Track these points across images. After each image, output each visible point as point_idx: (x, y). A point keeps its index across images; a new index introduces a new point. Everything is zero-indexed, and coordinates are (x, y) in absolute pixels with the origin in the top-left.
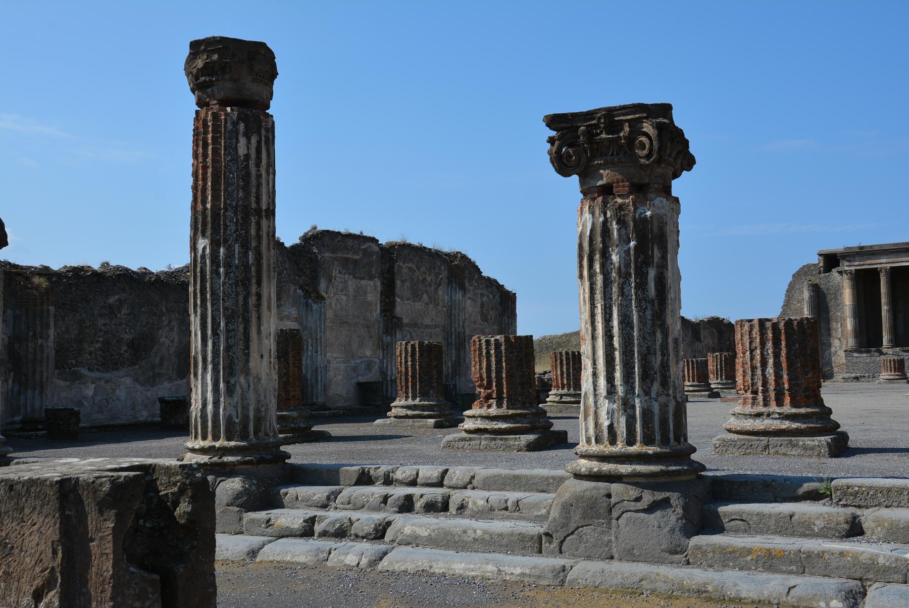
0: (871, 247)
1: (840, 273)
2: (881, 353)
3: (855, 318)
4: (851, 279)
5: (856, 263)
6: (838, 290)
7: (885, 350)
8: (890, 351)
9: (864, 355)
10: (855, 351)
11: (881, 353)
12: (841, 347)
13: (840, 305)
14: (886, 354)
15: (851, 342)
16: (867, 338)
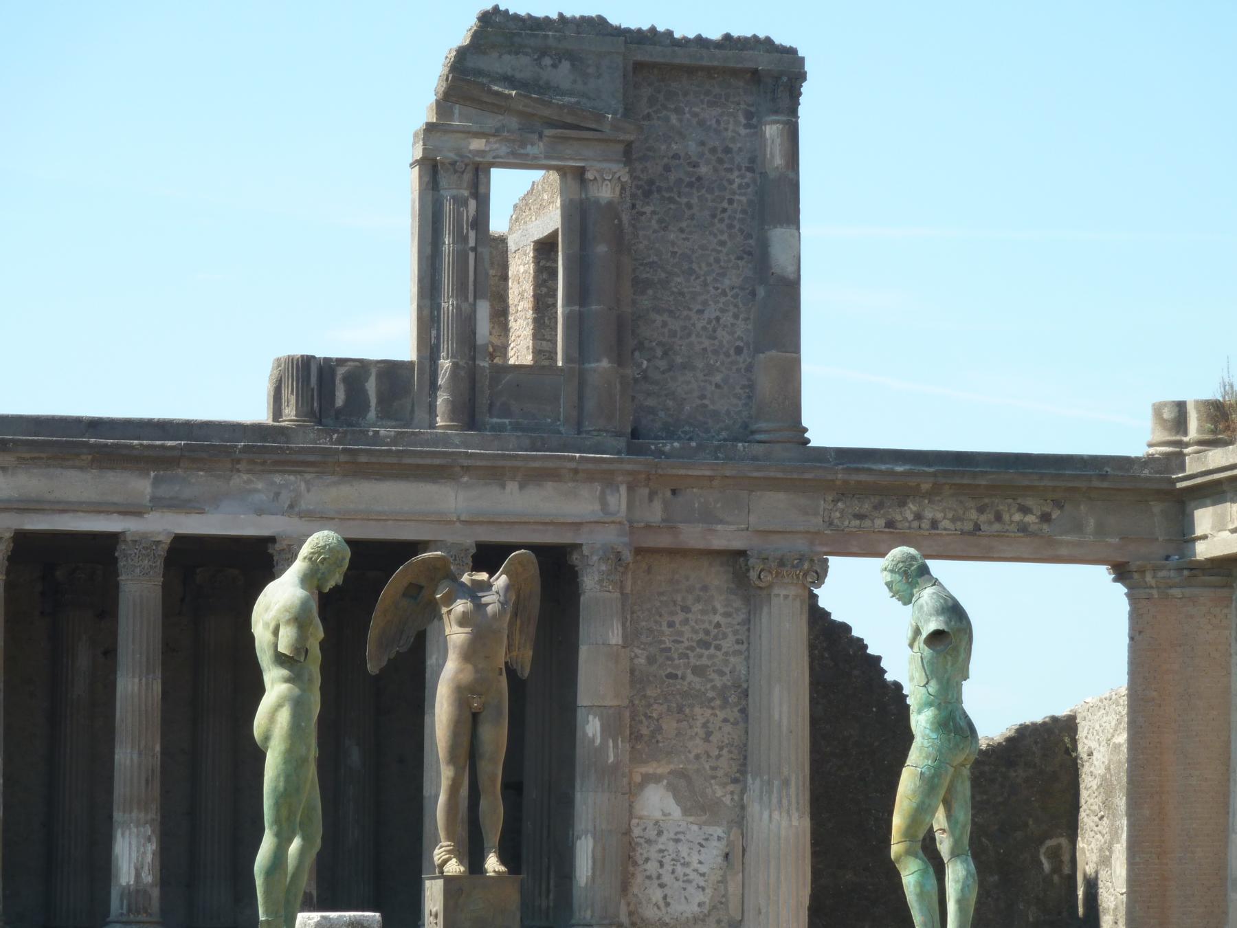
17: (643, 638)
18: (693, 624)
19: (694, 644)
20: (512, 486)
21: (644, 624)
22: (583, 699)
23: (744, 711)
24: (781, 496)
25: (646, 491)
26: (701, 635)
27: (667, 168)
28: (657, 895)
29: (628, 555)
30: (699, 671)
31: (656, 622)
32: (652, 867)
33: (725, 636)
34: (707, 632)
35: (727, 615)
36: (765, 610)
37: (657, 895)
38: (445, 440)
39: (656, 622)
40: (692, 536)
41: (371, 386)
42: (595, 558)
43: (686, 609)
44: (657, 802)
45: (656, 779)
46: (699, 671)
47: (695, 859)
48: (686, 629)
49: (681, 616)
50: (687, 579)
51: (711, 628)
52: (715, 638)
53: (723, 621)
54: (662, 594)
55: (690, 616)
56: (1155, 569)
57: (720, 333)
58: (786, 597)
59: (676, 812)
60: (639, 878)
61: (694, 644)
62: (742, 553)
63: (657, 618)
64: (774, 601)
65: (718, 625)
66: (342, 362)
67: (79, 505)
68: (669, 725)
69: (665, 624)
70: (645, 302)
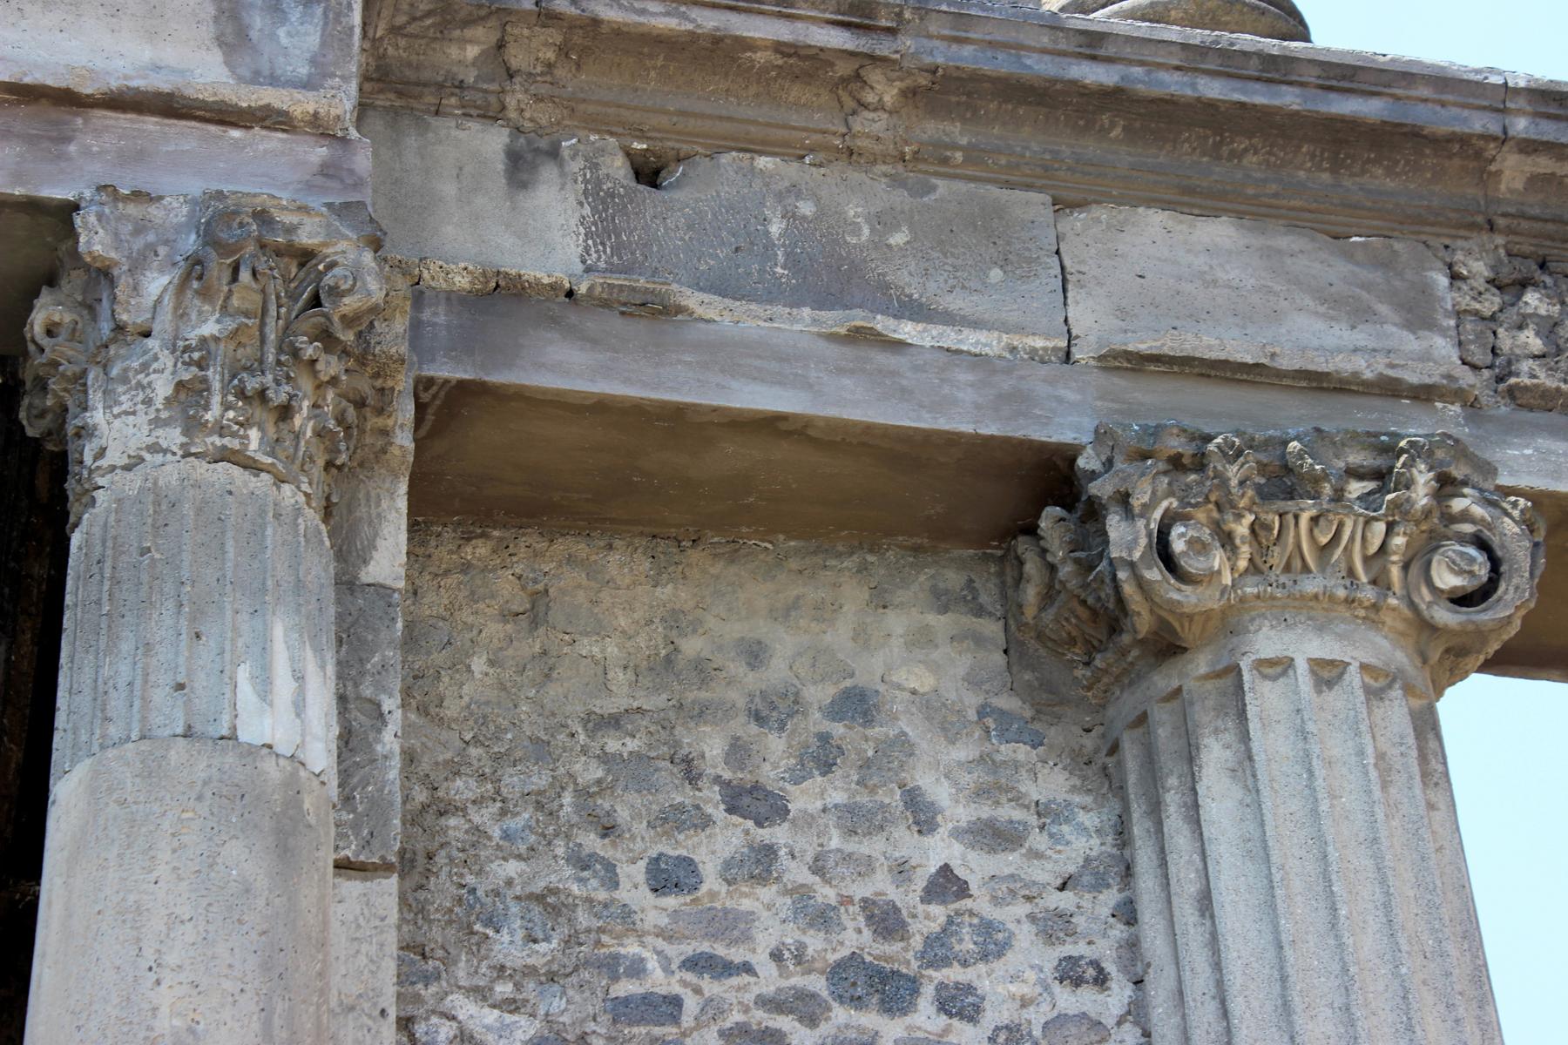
17: (508, 946)
18: (798, 873)
19: (818, 984)
21: (512, 868)
24: (1219, 232)
25: (493, 142)
26: (855, 937)
31: (583, 862)
33: (993, 944)
34: (886, 921)
35: (994, 836)
36: (1215, 754)
39: (583, 862)
40: (762, 362)
42: (157, 283)
43: (753, 801)
48: (758, 901)
49: (719, 843)
50: (755, 654)
51: (907, 898)
52: (938, 951)
53: (975, 866)
54: (613, 722)
55: (778, 834)
58: (1327, 674)
61: (818, 984)
63: (591, 841)
64: (1264, 698)
65: (946, 884)
69: (633, 874)
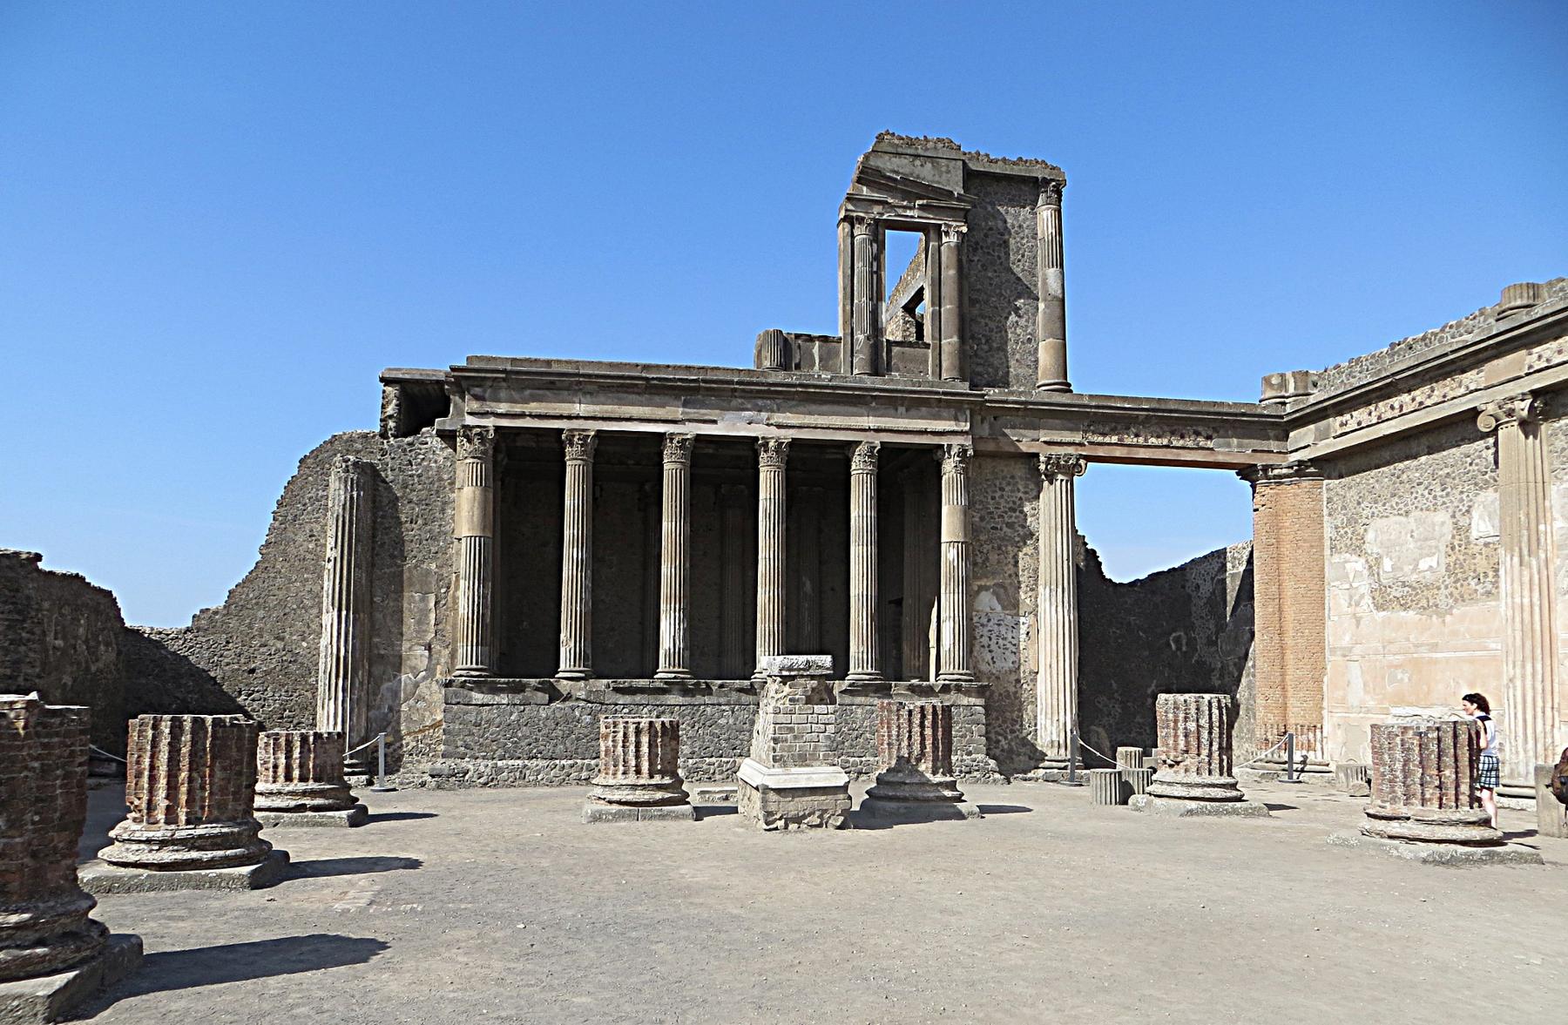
0: (548, 363)
1: (448, 437)
2: (555, 695)
3: (483, 581)
4: (480, 457)
5: (503, 408)
6: (440, 487)
7: (564, 686)
8: (580, 689)
9: (504, 699)
10: (479, 686)
11: (555, 695)
12: (430, 671)
13: (441, 537)
14: (568, 697)
15: (466, 658)
16: (515, 646)
20: (902, 410)
22: (944, 538)
23: (1036, 548)
27: (986, 236)
28: (988, 657)
29: (971, 452)
30: (1010, 525)
32: (985, 641)
37: (988, 657)
38: (861, 381)
41: (816, 351)
43: (1002, 489)
44: (986, 601)
45: (986, 588)
46: (1010, 525)
47: (1009, 636)
56: (1273, 467)
57: (1019, 331)
59: (999, 608)
60: (977, 647)
62: (1036, 455)
66: (798, 336)
67: (638, 418)
68: (993, 557)
70: (975, 312)
